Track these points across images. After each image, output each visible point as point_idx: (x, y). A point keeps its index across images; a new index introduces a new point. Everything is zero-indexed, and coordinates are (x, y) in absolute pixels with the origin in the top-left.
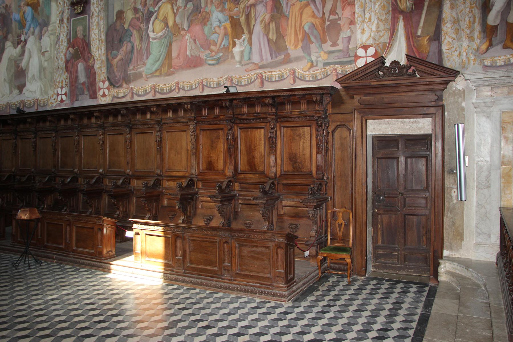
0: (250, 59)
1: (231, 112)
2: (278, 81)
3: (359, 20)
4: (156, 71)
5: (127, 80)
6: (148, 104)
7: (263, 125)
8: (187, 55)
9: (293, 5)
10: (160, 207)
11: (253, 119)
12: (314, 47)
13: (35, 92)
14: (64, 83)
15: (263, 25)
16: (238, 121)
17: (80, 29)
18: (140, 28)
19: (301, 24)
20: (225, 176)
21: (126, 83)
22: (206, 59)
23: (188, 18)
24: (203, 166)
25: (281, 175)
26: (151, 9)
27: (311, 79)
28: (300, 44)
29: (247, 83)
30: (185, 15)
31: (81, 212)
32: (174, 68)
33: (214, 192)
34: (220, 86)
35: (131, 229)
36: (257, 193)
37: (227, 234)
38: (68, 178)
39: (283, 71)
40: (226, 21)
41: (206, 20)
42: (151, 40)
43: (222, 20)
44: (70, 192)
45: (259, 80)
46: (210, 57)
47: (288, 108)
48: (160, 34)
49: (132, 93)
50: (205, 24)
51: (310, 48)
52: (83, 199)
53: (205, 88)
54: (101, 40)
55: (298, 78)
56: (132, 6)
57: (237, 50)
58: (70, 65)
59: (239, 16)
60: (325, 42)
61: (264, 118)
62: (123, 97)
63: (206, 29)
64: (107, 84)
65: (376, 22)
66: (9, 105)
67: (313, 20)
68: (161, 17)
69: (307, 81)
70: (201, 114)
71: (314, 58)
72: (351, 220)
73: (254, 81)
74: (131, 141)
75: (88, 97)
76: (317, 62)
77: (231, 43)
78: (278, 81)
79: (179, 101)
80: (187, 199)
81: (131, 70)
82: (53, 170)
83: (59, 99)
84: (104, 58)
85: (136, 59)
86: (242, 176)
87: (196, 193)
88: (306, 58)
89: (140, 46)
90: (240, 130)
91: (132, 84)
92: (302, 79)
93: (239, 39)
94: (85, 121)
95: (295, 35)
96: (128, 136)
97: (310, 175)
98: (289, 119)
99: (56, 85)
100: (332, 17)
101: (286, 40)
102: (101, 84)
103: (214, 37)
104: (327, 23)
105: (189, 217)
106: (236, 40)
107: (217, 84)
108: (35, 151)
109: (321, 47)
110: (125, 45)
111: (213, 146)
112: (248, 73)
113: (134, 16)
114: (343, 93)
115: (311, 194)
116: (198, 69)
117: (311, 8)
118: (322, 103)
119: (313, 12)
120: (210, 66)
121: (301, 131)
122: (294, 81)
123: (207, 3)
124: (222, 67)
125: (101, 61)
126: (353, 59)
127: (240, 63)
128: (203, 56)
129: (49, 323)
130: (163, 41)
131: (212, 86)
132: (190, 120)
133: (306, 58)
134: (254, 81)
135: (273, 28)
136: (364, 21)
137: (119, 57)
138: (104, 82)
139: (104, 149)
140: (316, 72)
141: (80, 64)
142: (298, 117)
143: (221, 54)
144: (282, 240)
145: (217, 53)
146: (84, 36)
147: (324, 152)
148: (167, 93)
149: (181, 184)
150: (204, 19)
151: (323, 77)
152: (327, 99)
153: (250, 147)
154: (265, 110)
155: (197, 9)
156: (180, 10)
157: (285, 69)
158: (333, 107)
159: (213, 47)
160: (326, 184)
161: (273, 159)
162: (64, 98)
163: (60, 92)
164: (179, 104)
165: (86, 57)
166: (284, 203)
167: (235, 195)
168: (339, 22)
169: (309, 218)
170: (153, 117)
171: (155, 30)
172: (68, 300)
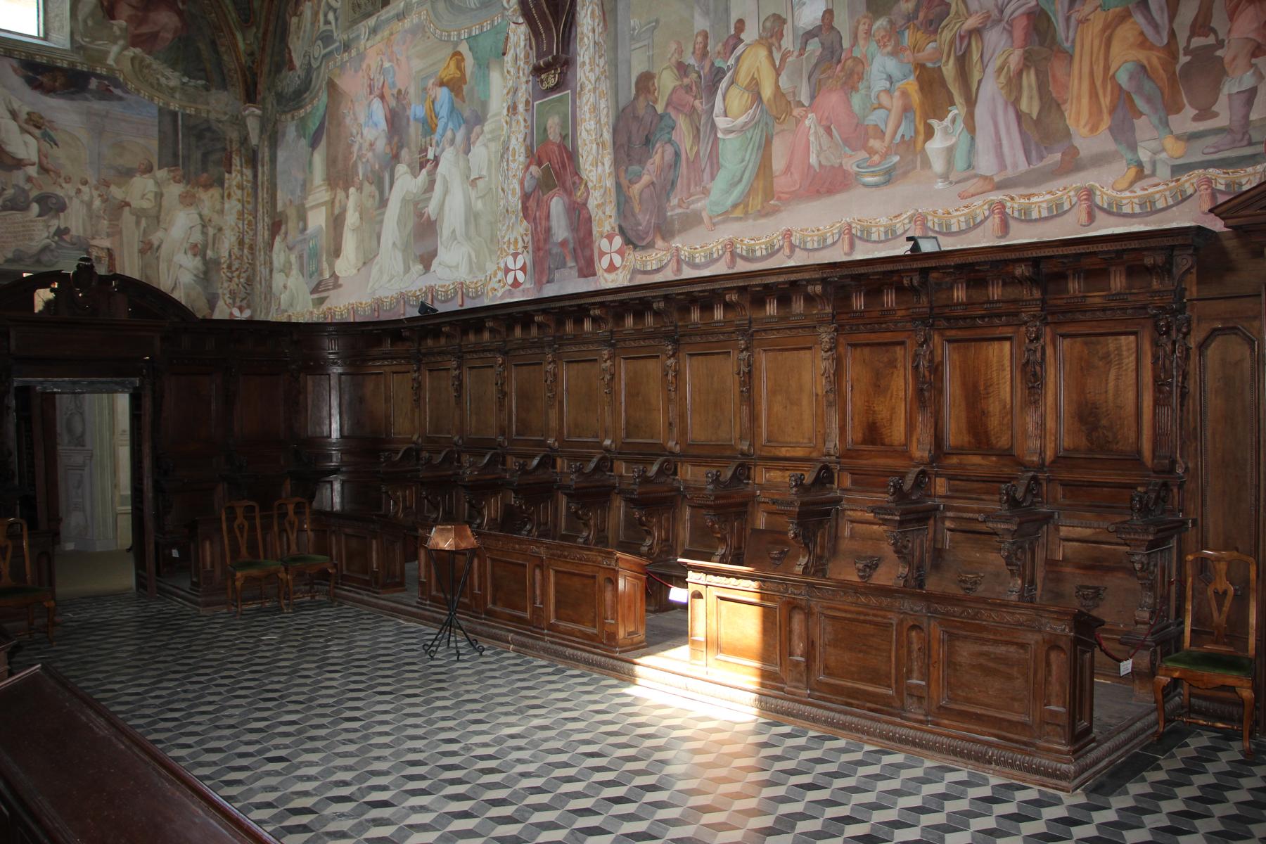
0: (970, 166)
1: (924, 300)
2: (1046, 219)
4: (735, 206)
5: (665, 230)
6: (717, 286)
7: (1008, 331)
8: (810, 166)
9: (1083, 21)
10: (749, 531)
11: (982, 317)
12: (1144, 127)
13: (457, 267)
14: (520, 244)
15: (1002, 79)
16: (944, 324)
17: (553, 122)
18: (693, 108)
19: (1107, 68)
20: (911, 459)
21: (663, 238)
22: (858, 174)
24: (853, 434)
25: (1057, 459)
28: (1106, 121)
29: (963, 226)
31: (563, 538)
32: (779, 199)
33: (884, 498)
34: (895, 237)
35: (683, 583)
36: (993, 505)
37: (919, 607)
38: (533, 457)
40: (905, 77)
42: (720, 135)
43: (896, 73)
44: (539, 491)
45: (996, 219)
46: (869, 166)
47: (1074, 286)
50: (854, 88)
51: (1132, 128)
52: (568, 508)
53: (857, 242)
54: (603, 143)
56: (673, 60)
57: (936, 145)
58: (532, 203)
59: (940, 60)
61: (1009, 313)
62: (657, 271)
63: (856, 100)
64: (618, 241)
66: (403, 298)
67: (1142, 56)
68: (743, 78)
69: (1126, 215)
70: (851, 306)
71: (1144, 155)
72: (1253, 584)
73: (982, 222)
74: (678, 374)
75: (575, 273)
77: (921, 128)
79: (793, 277)
80: (815, 516)
81: (674, 208)
82: (500, 439)
83: (510, 280)
84: (609, 183)
85: (685, 181)
86: (954, 460)
87: (838, 501)
89: (695, 149)
90: (947, 346)
91: (677, 239)
92: (1113, 211)
93: (941, 119)
94: (569, 327)
95: (1091, 98)
96: (671, 361)
97: (1135, 459)
98: (1079, 316)
99: (502, 250)
101: (1066, 114)
102: (604, 244)
103: (875, 118)
104: (1184, 59)
105: (820, 558)
106: (934, 122)
107: (886, 233)
108: (459, 397)
109: (1167, 125)
111: (878, 386)
112: (965, 202)
113: (678, 83)
114: (1231, 244)
115: (1139, 510)
116: (838, 198)
117: (1135, 23)
118: (1170, 272)
119: (1142, 33)
120: (867, 190)
121: (1112, 347)
122: (1091, 218)
123: (855, 37)
124: (901, 189)
127: (945, 177)
128: (850, 165)
129: (508, 791)
131: (874, 237)
132: (822, 322)
134: (982, 222)
135: (1030, 86)
137: (646, 179)
138: (610, 238)
139: (612, 393)
140: (1151, 190)
141: (555, 199)
142: (1104, 310)
143: (896, 159)
144: (1064, 629)
145: (885, 156)
146: (564, 137)
147: (1175, 400)
148: (763, 258)
149: (801, 478)
150: (851, 74)
151: (1170, 202)
152: (1184, 262)
153: (975, 386)
154: (1012, 292)
155: (832, 53)
157: (1066, 188)
158: (1201, 280)
159: (873, 143)
160: (1181, 486)
161: (1036, 418)
162: (521, 276)
163: (511, 266)
164: (793, 283)
165: (569, 184)
166: (1064, 531)
167: (936, 508)
169: (1132, 572)
170: (731, 316)
171: (731, 111)
172: (546, 740)
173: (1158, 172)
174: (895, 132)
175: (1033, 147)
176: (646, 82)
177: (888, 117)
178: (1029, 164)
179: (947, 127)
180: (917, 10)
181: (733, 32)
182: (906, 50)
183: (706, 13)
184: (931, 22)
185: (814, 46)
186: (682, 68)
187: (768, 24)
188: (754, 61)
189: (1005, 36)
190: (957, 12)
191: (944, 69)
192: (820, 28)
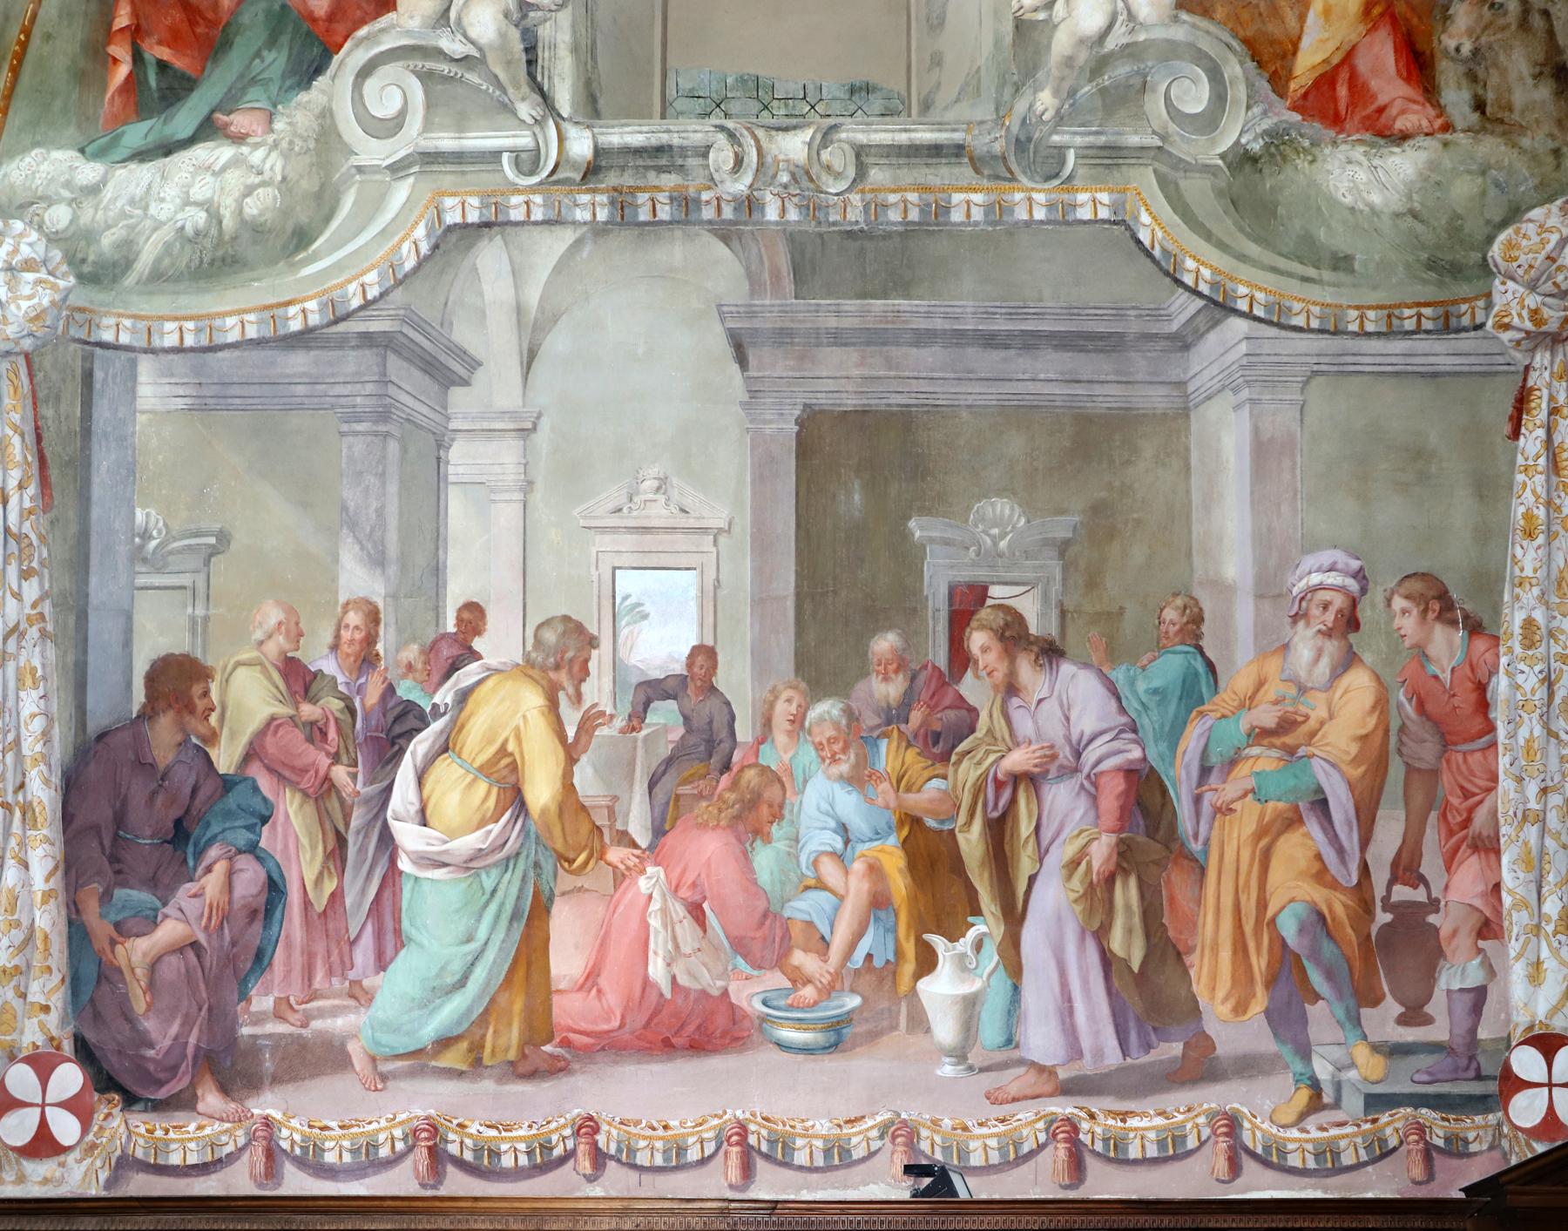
2: (1154, 1161)
4: (444, 1043)
5: (231, 1067)
8: (647, 983)
9: (1224, 810)
12: (1322, 1018)
15: (1077, 883)
19: (1262, 904)
21: (225, 1090)
22: (764, 1019)
23: (652, 785)
26: (407, 690)
27: (1311, 1164)
28: (1259, 1003)
29: (995, 1158)
30: (632, 764)
32: (566, 1043)
39: (1180, 1117)
40: (878, 835)
41: (765, 811)
42: (404, 864)
45: (1061, 1151)
46: (791, 1007)
48: (471, 841)
49: (272, 1154)
50: (760, 833)
51: (1304, 1020)
53: (760, 1164)
54: (27, 809)
55: (1252, 1154)
56: (272, 648)
57: (941, 990)
59: (953, 818)
60: (1376, 1001)
62: (203, 1169)
63: (765, 859)
64: (69, 1078)
67: (1319, 895)
69: (1292, 1171)
76: (1338, 1087)
77: (910, 949)
78: (1154, 1161)
81: (261, 1015)
85: (298, 959)
89: (330, 886)
92: (1272, 1159)
93: (953, 938)
95: (1235, 952)
100: (1401, 893)
101: (1192, 973)
102: (21, 1079)
103: (808, 906)
106: (938, 942)
107: (827, 1153)
109: (1357, 1022)
110: (220, 868)
117: (1308, 835)
119: (1319, 857)
120: (785, 1056)
122: (1235, 1169)
123: (767, 723)
124: (861, 1069)
125: (18, 936)
126: (1492, 1087)
127: (960, 1054)
130: (488, 883)
131: (801, 1158)
133: (1286, 1067)
134: (1032, 1154)
135: (1128, 907)
136: (1537, 929)
137: (170, 930)
138: (43, 1065)
140: (1334, 1132)
143: (853, 1001)
145: (828, 991)
148: (518, 1174)
151: (1364, 1157)
156: (603, 732)
157: (1190, 1109)
173: (1345, 1102)
174: (852, 946)
175: (1132, 1024)
176: (178, 683)
177: (837, 909)
178: (1125, 1054)
179: (962, 957)
180: (906, 703)
181: (451, 627)
182: (880, 779)
183: (378, 561)
184: (937, 737)
185: (665, 716)
186: (298, 678)
187: (550, 636)
188: (508, 712)
189: (1083, 804)
190: (990, 732)
191: (960, 837)
192: (682, 680)
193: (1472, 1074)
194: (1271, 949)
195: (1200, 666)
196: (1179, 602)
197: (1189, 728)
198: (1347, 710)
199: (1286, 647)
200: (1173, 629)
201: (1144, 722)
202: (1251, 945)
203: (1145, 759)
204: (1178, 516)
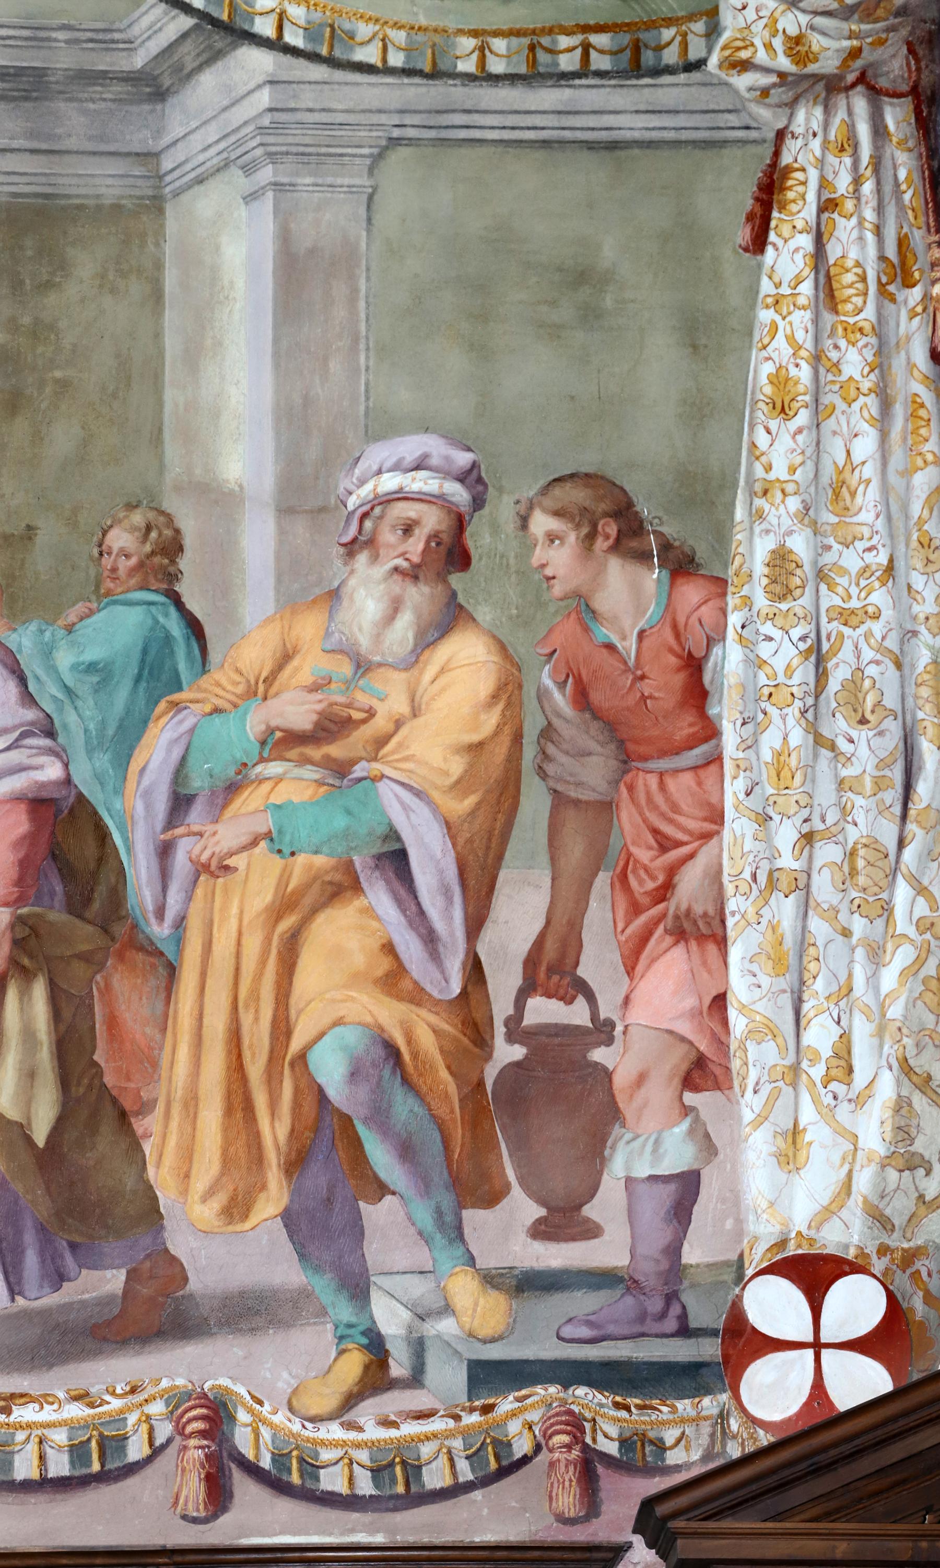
2: (63, 1485)
3: (755, 1058)
9: (215, 869)
12: (391, 1228)
27: (365, 1486)
39: (116, 1404)
51: (356, 1229)
55: (252, 1470)
60: (492, 1196)
65: (887, 1087)
67: (389, 1014)
69: (330, 1500)
71: (390, 1318)
76: (419, 1347)
78: (63, 1485)
88: (322, 1312)
95: (229, 1111)
100: (543, 1010)
101: (148, 1147)
109: (457, 1234)
117: (369, 912)
119: (389, 948)
122: (218, 1495)
126: (710, 1349)
133: (322, 1312)
135: (28, 1034)
140: (410, 1429)
151: (466, 1472)
168: (599, 1055)
178: (13, 1292)
193: (671, 1325)
194: (297, 1105)
195: (175, 626)
196: (138, 518)
197: (153, 730)
198: (448, 701)
199: (334, 595)
200: (124, 565)
201: (72, 723)
202: (260, 1100)
203: (68, 781)
204: (137, 375)
